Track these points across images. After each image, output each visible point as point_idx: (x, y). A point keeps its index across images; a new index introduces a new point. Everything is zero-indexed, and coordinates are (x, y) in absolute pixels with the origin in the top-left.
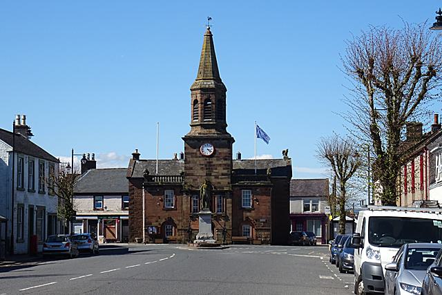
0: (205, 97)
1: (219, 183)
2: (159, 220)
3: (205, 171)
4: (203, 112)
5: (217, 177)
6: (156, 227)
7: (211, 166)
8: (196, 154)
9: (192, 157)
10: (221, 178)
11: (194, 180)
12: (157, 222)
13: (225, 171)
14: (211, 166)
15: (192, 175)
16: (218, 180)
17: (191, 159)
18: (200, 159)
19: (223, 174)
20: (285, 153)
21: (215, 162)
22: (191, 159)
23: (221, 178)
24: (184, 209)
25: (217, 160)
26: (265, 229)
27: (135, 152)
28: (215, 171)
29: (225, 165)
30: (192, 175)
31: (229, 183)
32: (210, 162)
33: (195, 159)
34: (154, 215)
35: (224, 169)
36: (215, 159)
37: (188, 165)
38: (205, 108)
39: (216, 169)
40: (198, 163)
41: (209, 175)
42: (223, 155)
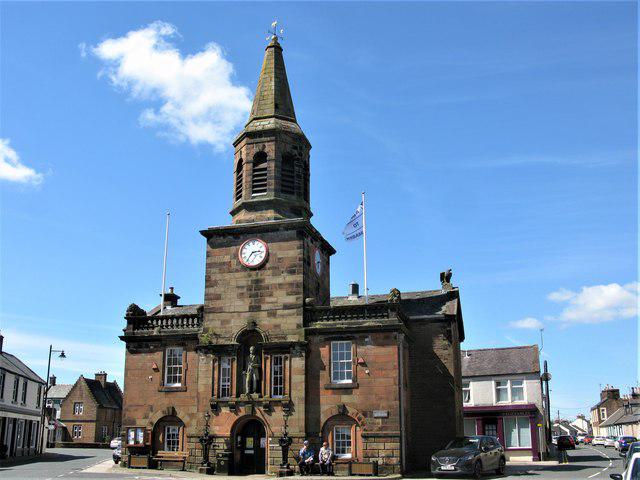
0: (255, 149)
1: (277, 326)
2: (151, 414)
3: (248, 301)
4: (249, 179)
5: (272, 314)
6: (144, 429)
9: (222, 272)
10: (283, 316)
12: (146, 417)
13: (291, 299)
15: (221, 310)
16: (274, 321)
17: (218, 277)
18: (237, 275)
19: (286, 307)
20: (445, 278)
21: (269, 279)
22: (218, 277)
23: (283, 316)
24: (201, 389)
25: (274, 275)
26: (385, 436)
27: (169, 291)
28: (268, 299)
29: (291, 284)
30: (221, 310)
31: (298, 326)
32: (257, 281)
33: (228, 276)
34: (141, 403)
35: (288, 294)
36: (269, 272)
37: (211, 290)
38: (254, 171)
39: (271, 295)
40: (233, 283)
41: (255, 308)
42: (287, 264)
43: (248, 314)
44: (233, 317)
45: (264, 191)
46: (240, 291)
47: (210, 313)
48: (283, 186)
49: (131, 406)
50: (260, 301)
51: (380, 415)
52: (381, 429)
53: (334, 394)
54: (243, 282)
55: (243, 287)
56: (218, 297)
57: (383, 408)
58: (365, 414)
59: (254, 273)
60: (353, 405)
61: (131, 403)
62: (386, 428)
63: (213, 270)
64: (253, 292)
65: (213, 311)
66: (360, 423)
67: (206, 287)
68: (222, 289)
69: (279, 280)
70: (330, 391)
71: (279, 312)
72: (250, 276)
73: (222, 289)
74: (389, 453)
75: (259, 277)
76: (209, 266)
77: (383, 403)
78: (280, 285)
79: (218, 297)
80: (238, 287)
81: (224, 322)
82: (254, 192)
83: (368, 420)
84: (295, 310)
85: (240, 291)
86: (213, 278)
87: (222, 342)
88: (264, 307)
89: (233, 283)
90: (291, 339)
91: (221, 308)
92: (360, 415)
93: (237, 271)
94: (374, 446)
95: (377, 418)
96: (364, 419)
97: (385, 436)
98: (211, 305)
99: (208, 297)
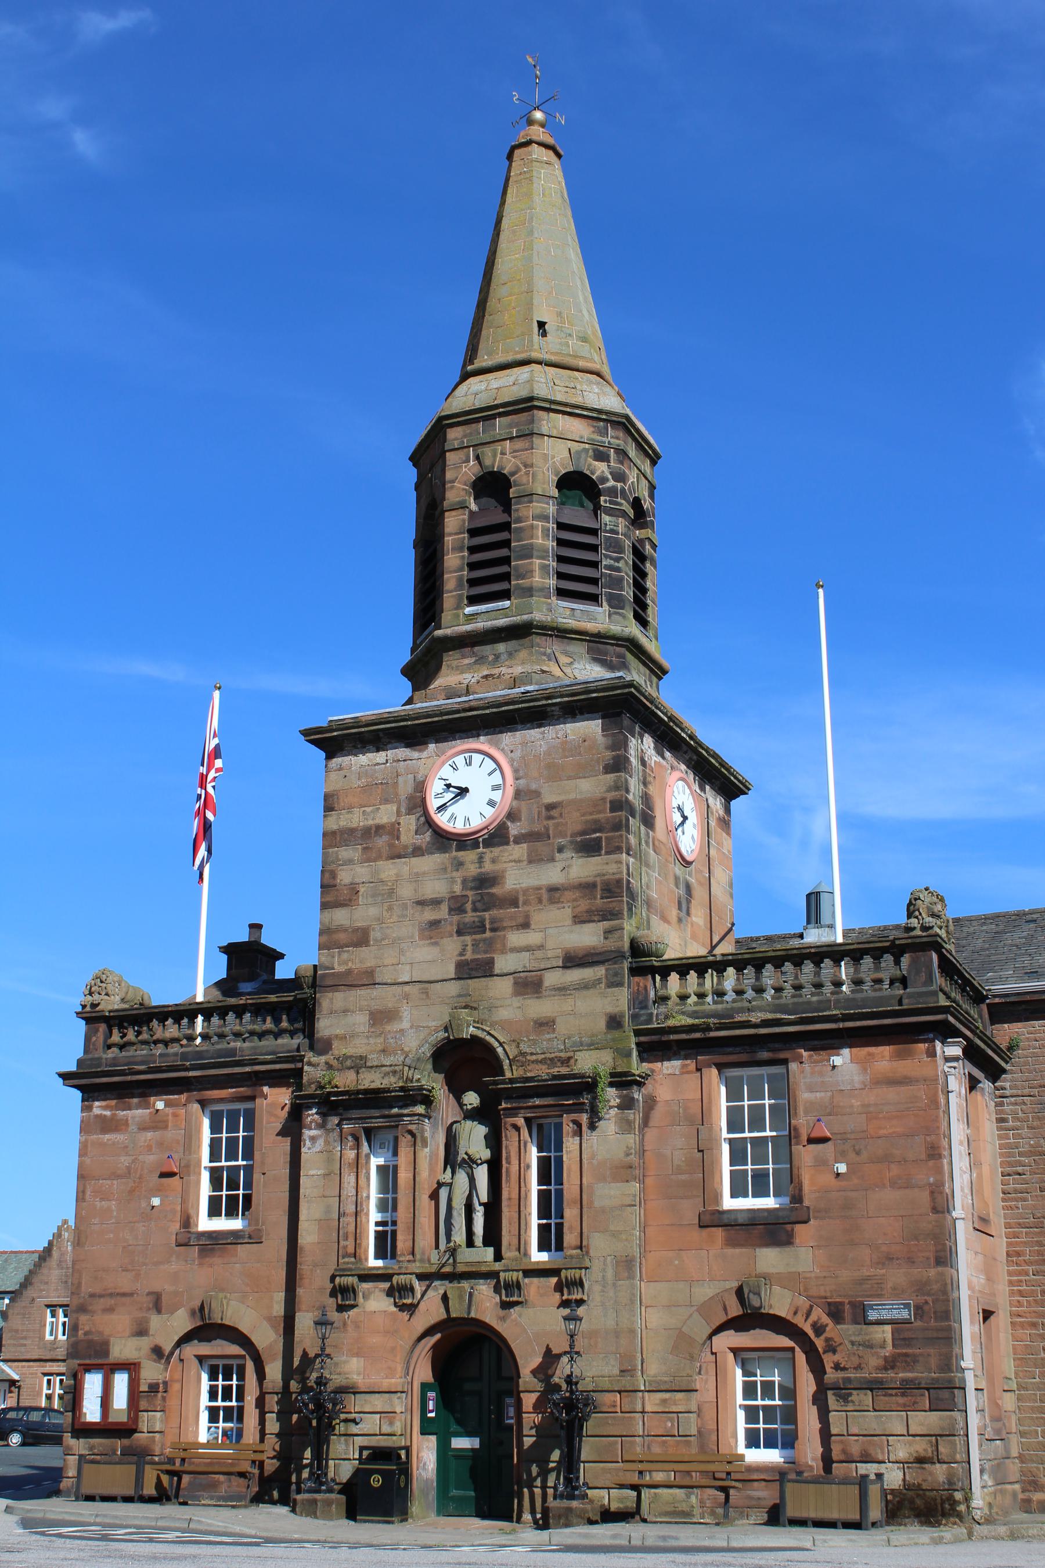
1: (545, 1024)
2: (155, 1321)
7: (487, 903)
8: (393, 830)
9: (370, 856)
10: (562, 990)
11: (380, 1017)
12: (141, 1331)
14: (487, 903)
15: (368, 980)
19: (573, 960)
23: (562, 990)
25: (534, 859)
26: (907, 1388)
28: (515, 938)
29: (587, 888)
30: (368, 980)
31: (614, 1022)
32: (484, 882)
33: (389, 870)
34: (124, 1282)
35: (579, 920)
36: (519, 851)
37: (340, 916)
39: (525, 925)
40: (406, 892)
42: (574, 821)
43: (453, 988)
44: (406, 997)
45: (505, 595)
46: (429, 915)
47: (334, 987)
48: (561, 576)
49: (92, 1296)
50: (490, 944)
51: (885, 1315)
52: (890, 1364)
53: (731, 1243)
54: (436, 887)
55: (436, 902)
56: (361, 938)
57: (897, 1292)
58: (836, 1313)
59: (469, 856)
60: (791, 1281)
61: (97, 1289)
62: (911, 1362)
63: (345, 853)
64: (470, 917)
65: (347, 982)
66: (819, 1343)
67: (325, 906)
68: (373, 911)
69: (552, 874)
70: (719, 1233)
71: (551, 979)
72: (459, 865)
73: (373, 911)
74: (921, 1447)
75: (488, 867)
76: (332, 839)
77: (897, 1276)
78: (553, 889)
79: (361, 938)
80: (421, 903)
81: (380, 1017)
82: (473, 600)
83: (845, 1332)
84: (600, 971)
85: (429, 915)
86: (344, 877)
87: (371, 1080)
88: (504, 963)
89: (406, 892)
90: (586, 1062)
91: (370, 973)
92: (819, 1314)
93: (418, 851)
94: (870, 1421)
95: (879, 1323)
96: (832, 1330)
97: (907, 1388)
98: (339, 962)
99: (329, 938)
